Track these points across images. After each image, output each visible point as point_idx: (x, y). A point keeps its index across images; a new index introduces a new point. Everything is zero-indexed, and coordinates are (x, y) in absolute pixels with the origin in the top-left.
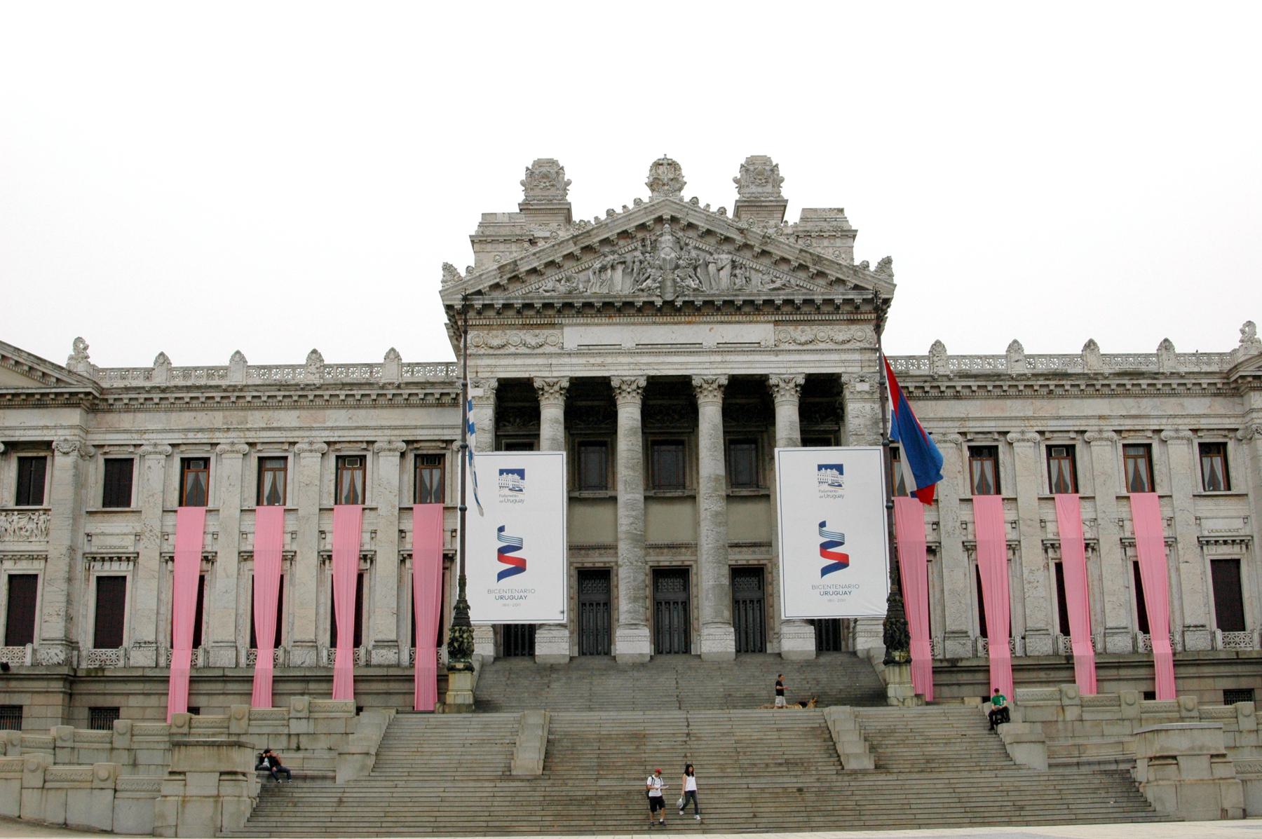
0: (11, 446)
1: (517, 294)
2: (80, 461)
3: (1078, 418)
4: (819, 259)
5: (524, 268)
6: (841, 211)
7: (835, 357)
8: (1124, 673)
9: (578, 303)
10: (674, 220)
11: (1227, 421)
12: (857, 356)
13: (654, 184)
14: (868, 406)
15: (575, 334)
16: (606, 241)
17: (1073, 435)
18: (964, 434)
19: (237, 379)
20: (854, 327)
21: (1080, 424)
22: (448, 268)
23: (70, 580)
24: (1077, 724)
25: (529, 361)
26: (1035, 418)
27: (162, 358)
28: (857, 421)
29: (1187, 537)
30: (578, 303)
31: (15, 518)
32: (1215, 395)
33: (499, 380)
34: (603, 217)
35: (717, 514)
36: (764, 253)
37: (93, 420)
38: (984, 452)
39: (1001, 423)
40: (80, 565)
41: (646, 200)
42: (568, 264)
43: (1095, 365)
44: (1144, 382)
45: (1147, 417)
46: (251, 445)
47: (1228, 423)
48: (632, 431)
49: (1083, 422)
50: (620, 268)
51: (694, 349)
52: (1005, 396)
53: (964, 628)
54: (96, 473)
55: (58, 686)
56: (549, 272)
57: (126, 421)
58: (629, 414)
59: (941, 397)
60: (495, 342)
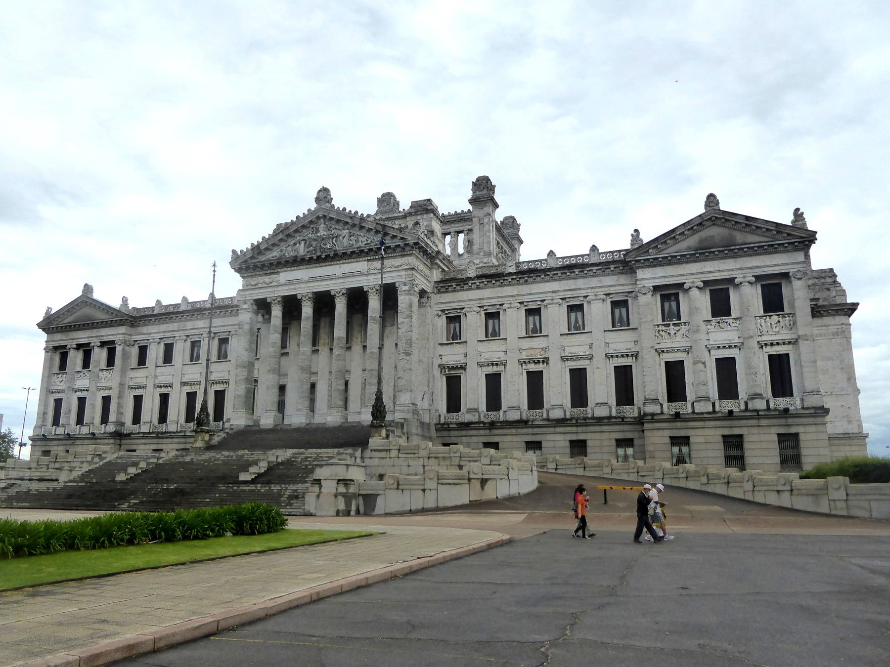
0: (103, 344)
1: (263, 258)
2: (127, 348)
3: (541, 293)
4: (384, 226)
5: (262, 247)
6: (429, 200)
7: (394, 274)
8: (559, 430)
9: (283, 261)
10: (325, 216)
11: (627, 287)
12: (404, 273)
13: (318, 200)
14: (407, 297)
15: (285, 276)
16: (296, 231)
17: (539, 303)
18: (482, 307)
19: (183, 308)
20: (404, 259)
21: (543, 297)
22: (234, 251)
23: (120, 397)
24: (396, 459)
25: (266, 290)
26: (517, 295)
27: (158, 302)
28: (404, 305)
29: (599, 354)
30: (283, 261)
31: (105, 372)
32: (620, 273)
33: (256, 300)
34: (295, 220)
35: (338, 355)
36: (362, 228)
37: (132, 330)
38: (493, 316)
39: (500, 299)
40: (127, 391)
41: (313, 209)
42: (282, 244)
43: (552, 264)
44: (577, 271)
45: (580, 289)
46: (187, 336)
47: (627, 289)
48: (307, 319)
49: (544, 295)
50: (303, 243)
51: (332, 277)
52: (502, 285)
53: (476, 407)
54: (135, 351)
55: (112, 441)
56: (275, 248)
57: (144, 330)
58: (307, 310)
59: (470, 289)
60: (253, 283)
